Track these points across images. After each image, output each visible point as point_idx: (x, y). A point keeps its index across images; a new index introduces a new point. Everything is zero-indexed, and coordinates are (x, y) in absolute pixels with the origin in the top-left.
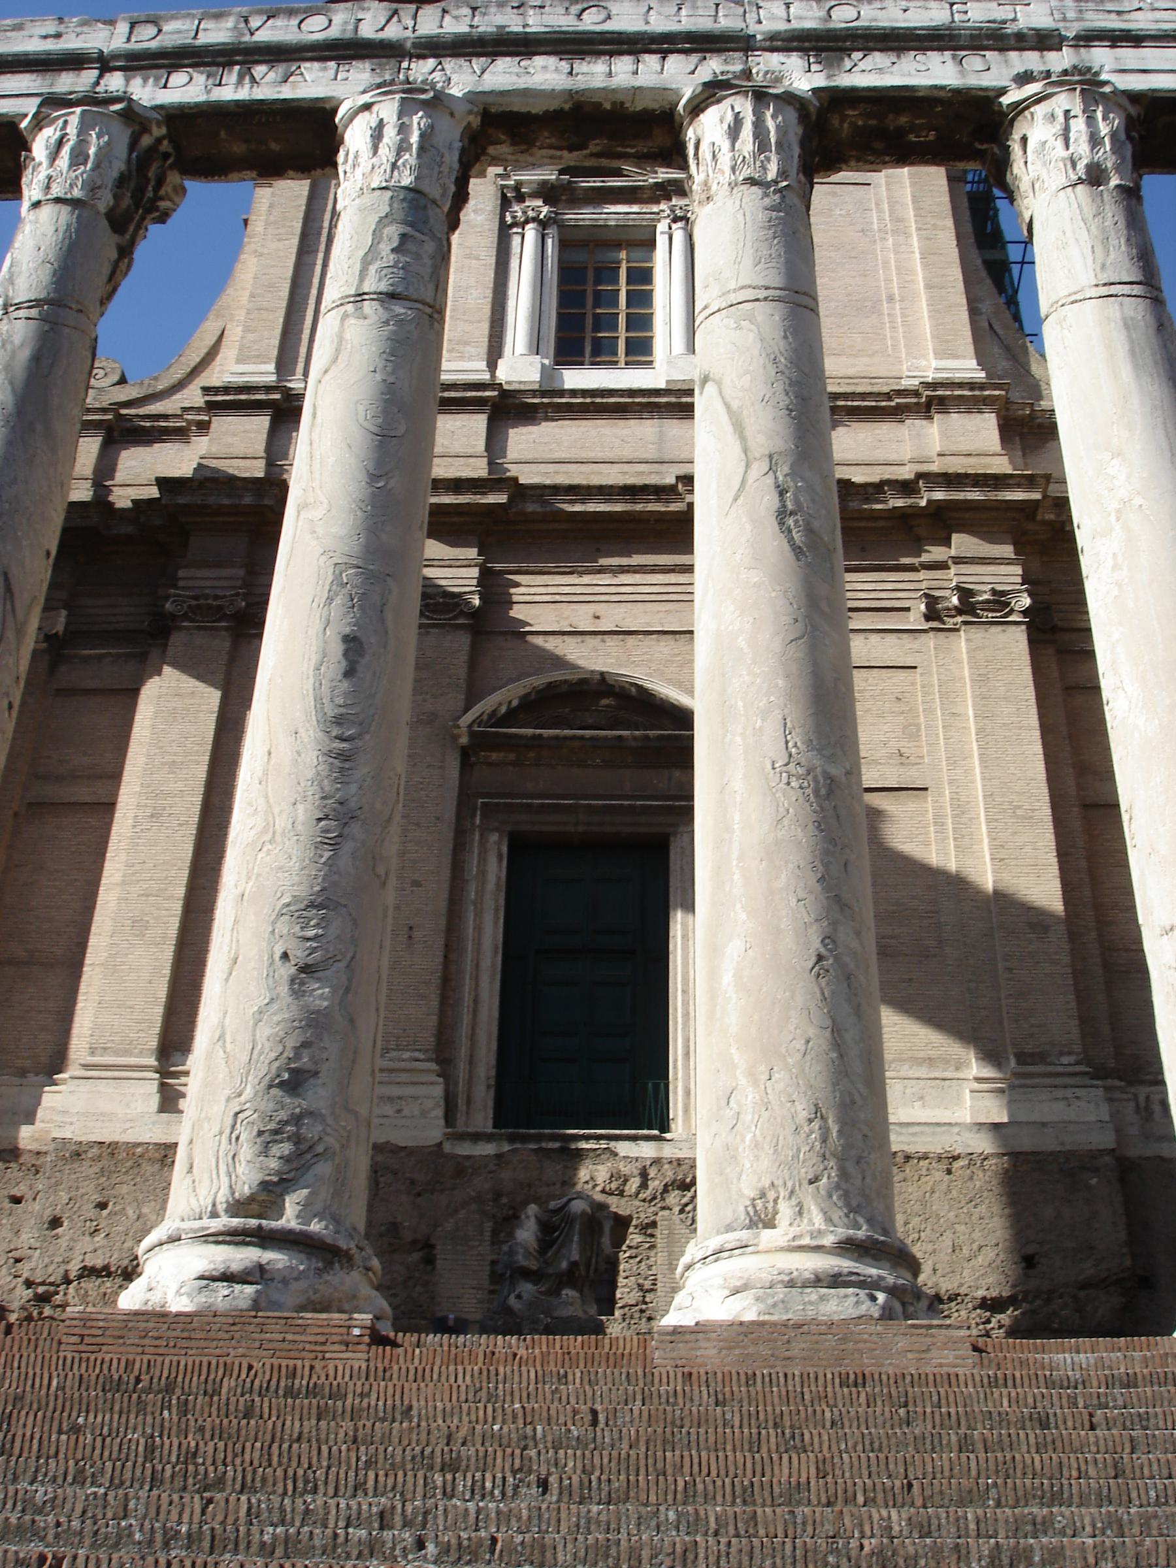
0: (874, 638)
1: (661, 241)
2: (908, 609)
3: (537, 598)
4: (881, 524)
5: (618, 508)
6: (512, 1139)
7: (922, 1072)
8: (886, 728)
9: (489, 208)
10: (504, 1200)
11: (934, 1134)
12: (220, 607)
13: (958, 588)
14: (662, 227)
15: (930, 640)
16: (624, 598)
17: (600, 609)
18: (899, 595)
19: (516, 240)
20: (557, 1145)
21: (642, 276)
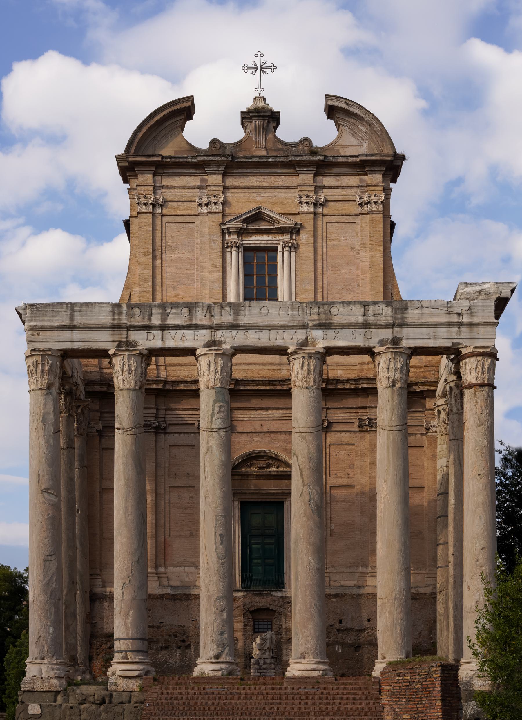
0: (343, 434)
1: (280, 255)
2: (353, 422)
3: (244, 419)
4: (348, 391)
5: (268, 388)
6: (246, 591)
7: (348, 570)
8: (345, 465)
9: (218, 239)
10: (246, 607)
11: (349, 589)
12: (150, 425)
13: (369, 418)
14: (280, 248)
15: (359, 435)
16: (270, 419)
17: (263, 422)
18: (352, 417)
19: (228, 255)
20: (257, 593)
21: (274, 267)
